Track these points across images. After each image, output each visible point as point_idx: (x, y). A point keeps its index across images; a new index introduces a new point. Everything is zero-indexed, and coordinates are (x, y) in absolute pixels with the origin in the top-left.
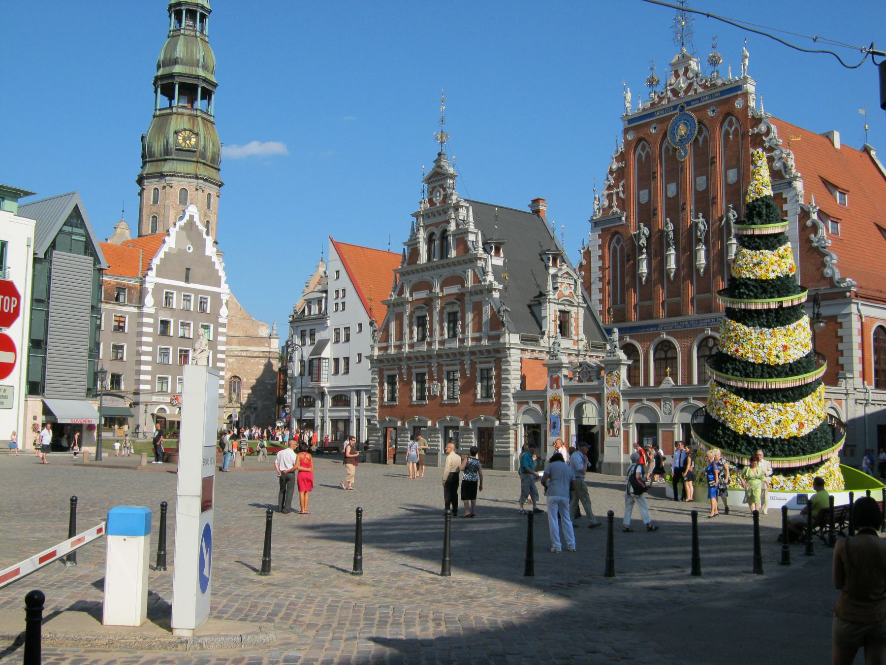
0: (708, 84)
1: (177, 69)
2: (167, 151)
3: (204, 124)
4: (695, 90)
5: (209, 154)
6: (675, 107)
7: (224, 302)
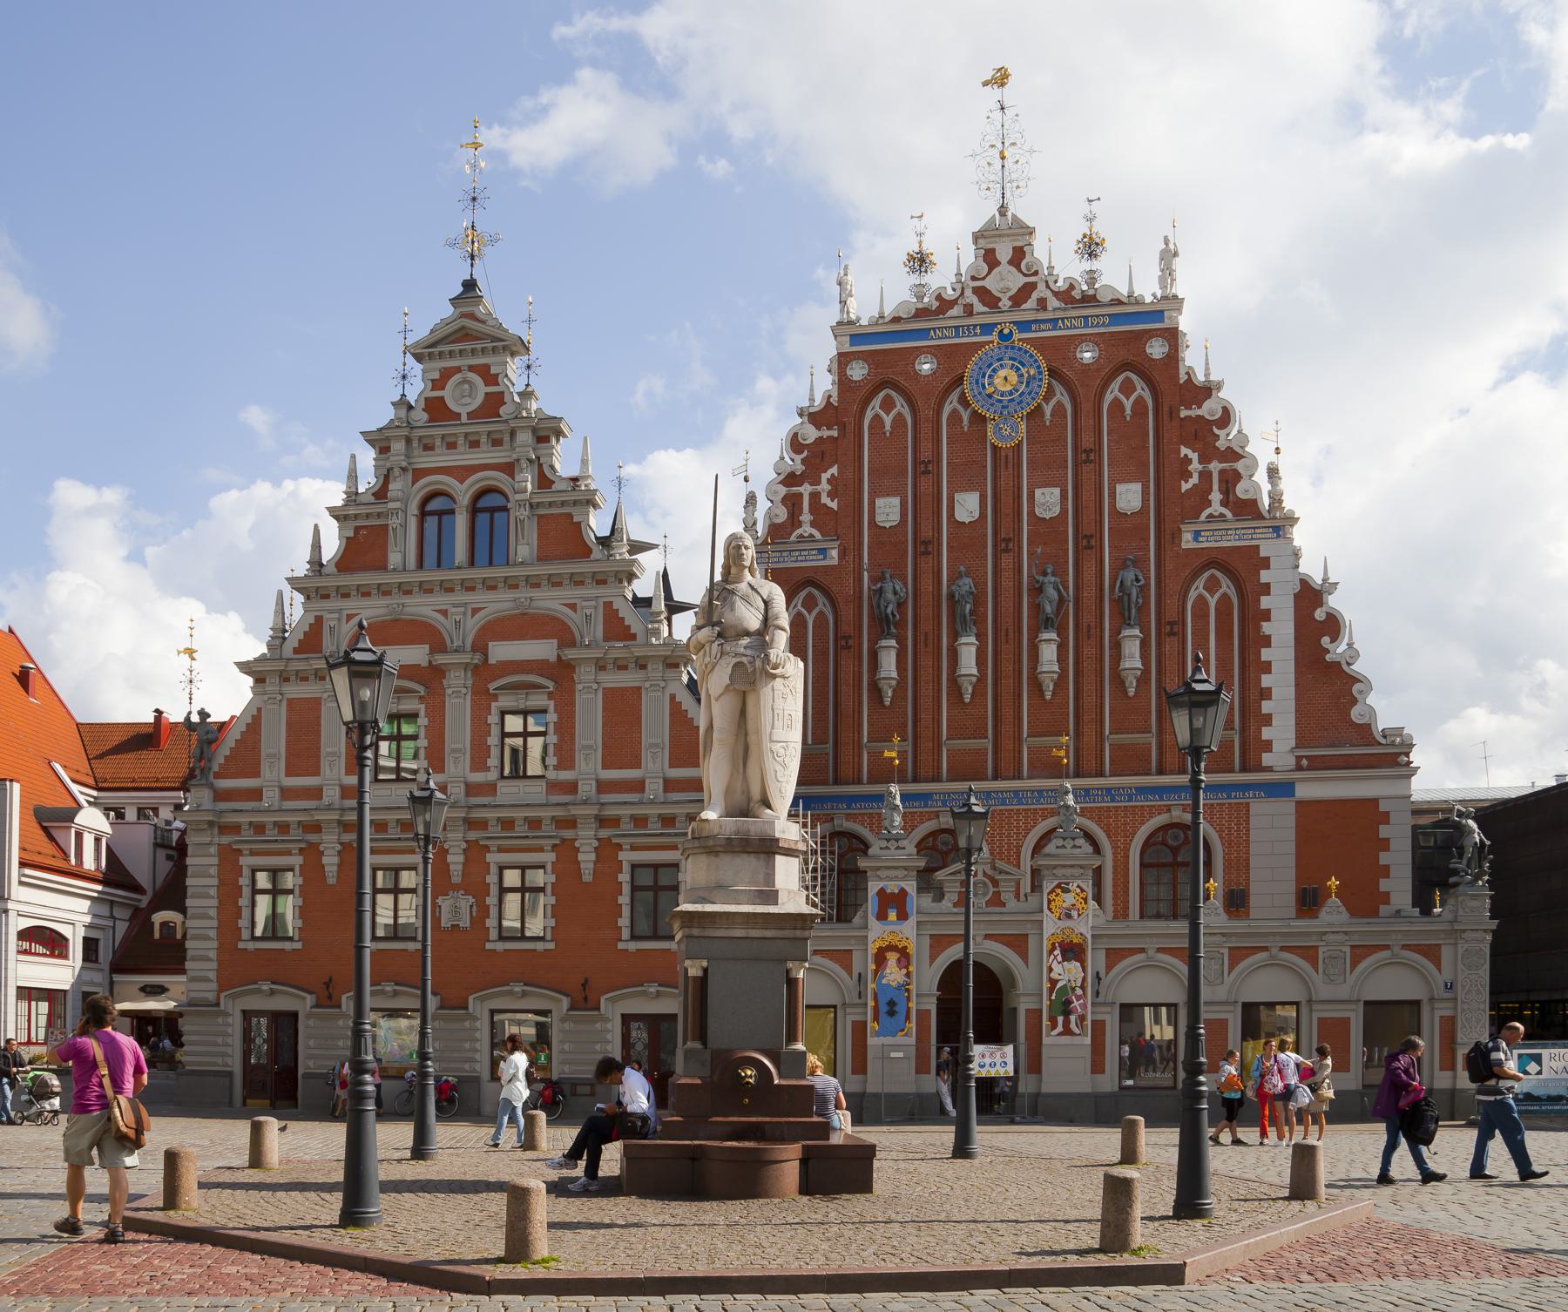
0: (1076, 294)
4: (1042, 303)
6: (987, 328)
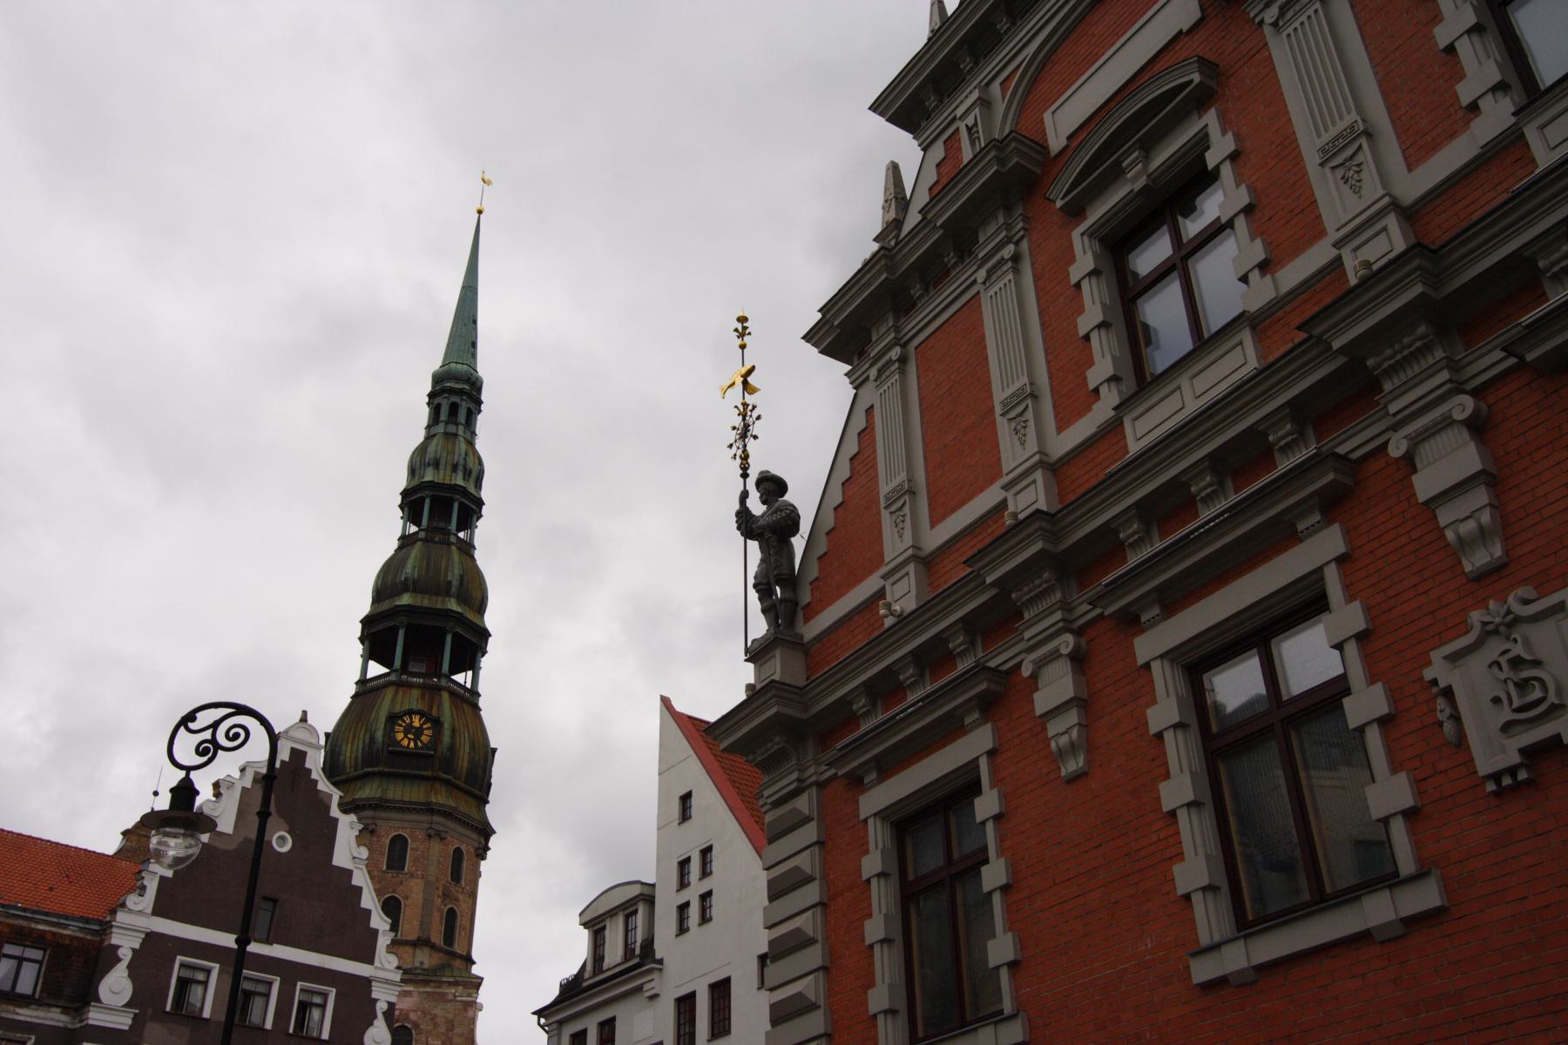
1: (405, 599)
2: (370, 757)
3: (453, 704)
5: (463, 763)
7: (381, 1007)
